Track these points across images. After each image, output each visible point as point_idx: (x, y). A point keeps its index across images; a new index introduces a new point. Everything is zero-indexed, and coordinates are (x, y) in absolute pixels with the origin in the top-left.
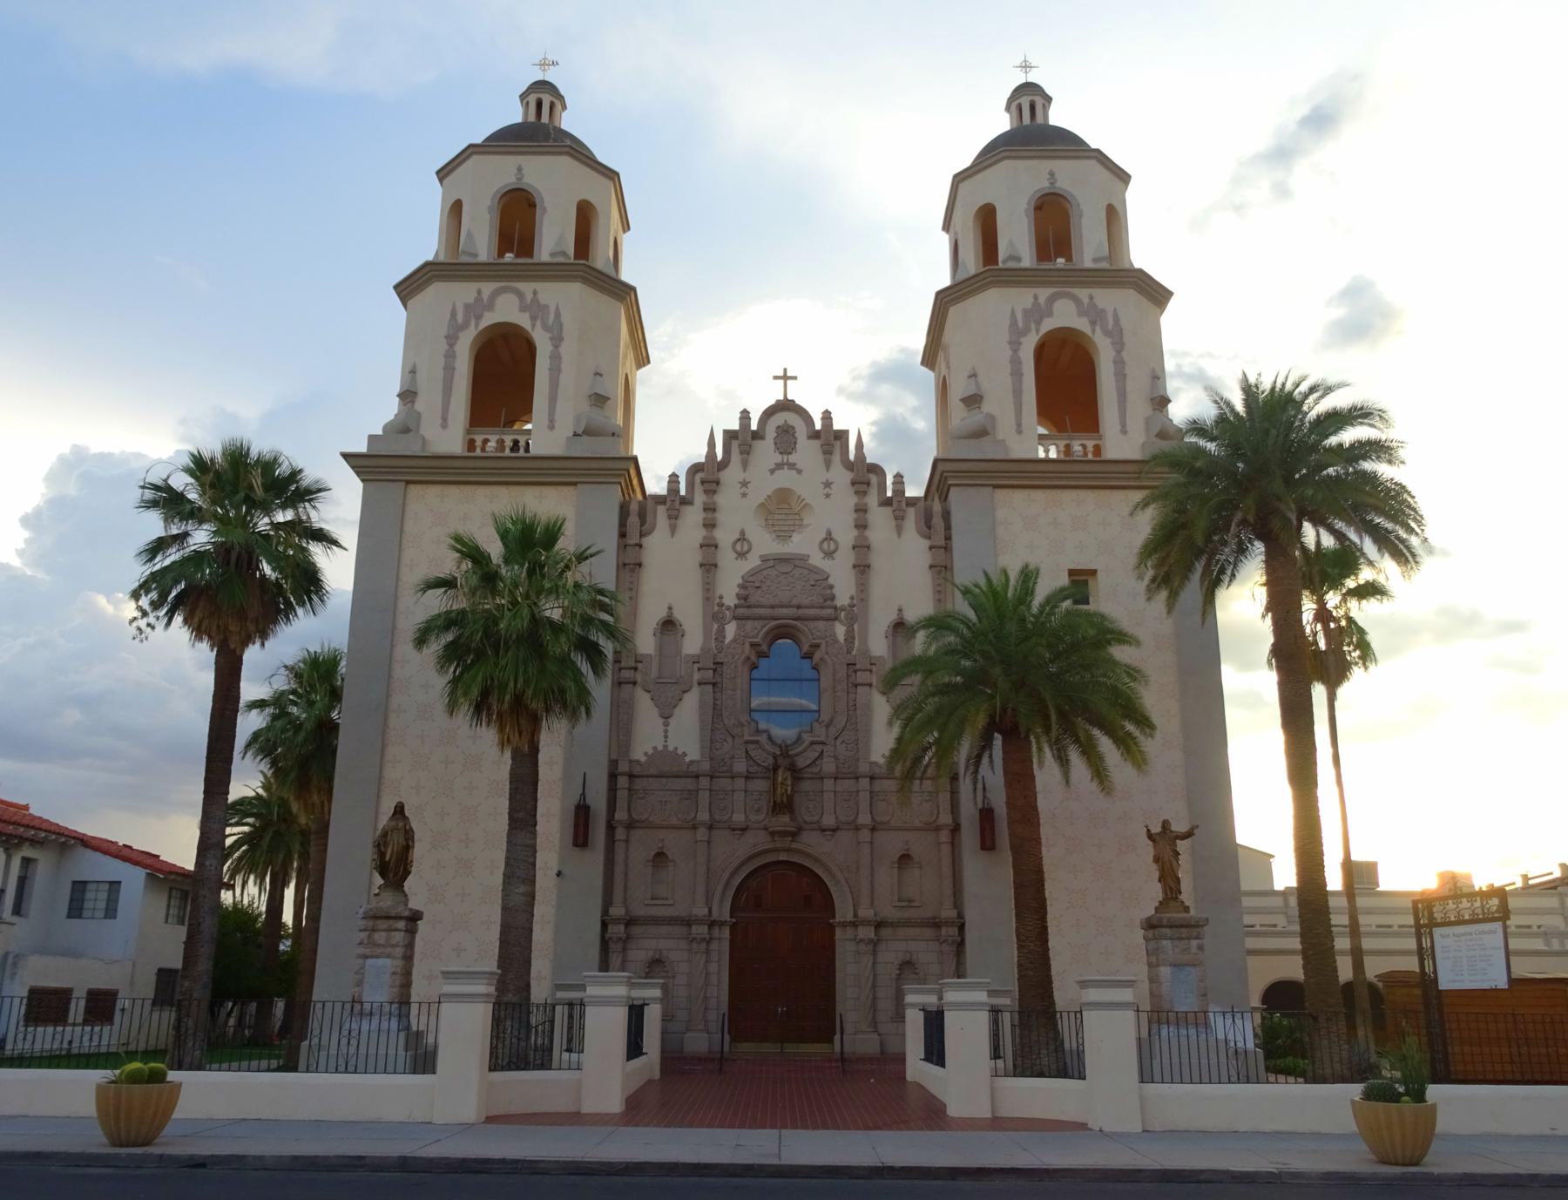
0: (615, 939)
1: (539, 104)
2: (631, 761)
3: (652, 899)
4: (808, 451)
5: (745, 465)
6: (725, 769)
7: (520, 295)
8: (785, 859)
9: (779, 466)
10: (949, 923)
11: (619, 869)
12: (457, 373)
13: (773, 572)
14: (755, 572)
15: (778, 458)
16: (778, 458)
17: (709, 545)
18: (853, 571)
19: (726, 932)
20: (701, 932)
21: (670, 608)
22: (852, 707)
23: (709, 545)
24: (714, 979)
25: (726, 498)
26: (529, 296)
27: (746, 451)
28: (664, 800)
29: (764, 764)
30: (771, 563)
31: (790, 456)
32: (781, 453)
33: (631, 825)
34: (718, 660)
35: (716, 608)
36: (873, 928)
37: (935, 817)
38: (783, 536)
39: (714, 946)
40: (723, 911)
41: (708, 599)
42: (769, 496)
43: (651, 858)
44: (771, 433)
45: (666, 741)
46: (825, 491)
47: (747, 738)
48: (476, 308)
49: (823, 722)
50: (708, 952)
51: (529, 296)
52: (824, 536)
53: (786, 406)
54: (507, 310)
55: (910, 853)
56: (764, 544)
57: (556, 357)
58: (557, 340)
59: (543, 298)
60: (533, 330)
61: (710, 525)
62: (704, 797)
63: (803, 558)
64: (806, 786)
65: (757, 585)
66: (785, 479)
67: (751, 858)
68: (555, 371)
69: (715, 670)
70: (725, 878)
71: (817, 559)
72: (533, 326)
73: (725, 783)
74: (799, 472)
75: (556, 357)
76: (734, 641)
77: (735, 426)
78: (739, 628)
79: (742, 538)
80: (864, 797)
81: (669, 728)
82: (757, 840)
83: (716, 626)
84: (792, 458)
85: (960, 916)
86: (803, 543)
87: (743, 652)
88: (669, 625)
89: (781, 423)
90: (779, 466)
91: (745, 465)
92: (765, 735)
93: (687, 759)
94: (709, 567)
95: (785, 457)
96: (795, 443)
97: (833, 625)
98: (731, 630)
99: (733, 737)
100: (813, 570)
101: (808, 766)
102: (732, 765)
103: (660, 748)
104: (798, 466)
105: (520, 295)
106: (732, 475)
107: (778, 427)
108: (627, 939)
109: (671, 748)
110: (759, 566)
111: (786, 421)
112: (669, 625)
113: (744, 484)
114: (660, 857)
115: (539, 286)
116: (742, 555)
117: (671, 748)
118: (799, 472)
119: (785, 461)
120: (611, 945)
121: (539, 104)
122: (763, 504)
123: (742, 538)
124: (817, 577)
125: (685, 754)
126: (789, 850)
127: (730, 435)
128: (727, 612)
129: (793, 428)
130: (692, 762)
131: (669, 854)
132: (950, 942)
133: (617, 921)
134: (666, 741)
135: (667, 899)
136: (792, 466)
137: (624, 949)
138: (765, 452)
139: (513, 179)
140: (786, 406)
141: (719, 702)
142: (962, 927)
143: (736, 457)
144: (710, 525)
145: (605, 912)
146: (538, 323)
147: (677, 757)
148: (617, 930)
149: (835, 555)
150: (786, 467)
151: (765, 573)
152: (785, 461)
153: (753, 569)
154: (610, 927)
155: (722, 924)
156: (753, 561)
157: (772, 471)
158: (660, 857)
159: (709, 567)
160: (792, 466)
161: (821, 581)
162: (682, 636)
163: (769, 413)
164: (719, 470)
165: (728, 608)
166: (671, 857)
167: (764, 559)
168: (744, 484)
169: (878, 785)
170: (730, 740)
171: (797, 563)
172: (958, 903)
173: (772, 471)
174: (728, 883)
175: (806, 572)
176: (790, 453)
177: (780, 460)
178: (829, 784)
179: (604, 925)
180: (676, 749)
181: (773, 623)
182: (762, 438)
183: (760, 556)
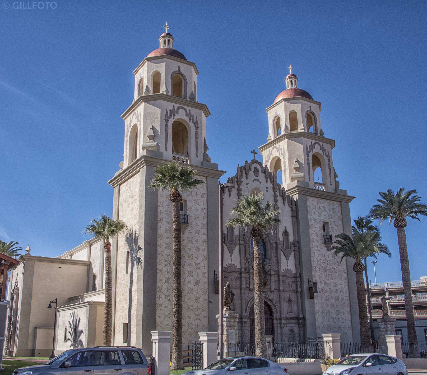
4: (262, 177)
9: (255, 180)
12: (310, 165)
16: (255, 177)
31: (258, 177)
32: (256, 176)
74: (260, 182)
81: (232, 257)
84: (258, 178)
99: (249, 262)
113: (247, 184)
118: (260, 182)
134: (231, 262)
136: (258, 180)
140: (255, 161)
157: (254, 181)
168: (247, 184)
170: (248, 263)
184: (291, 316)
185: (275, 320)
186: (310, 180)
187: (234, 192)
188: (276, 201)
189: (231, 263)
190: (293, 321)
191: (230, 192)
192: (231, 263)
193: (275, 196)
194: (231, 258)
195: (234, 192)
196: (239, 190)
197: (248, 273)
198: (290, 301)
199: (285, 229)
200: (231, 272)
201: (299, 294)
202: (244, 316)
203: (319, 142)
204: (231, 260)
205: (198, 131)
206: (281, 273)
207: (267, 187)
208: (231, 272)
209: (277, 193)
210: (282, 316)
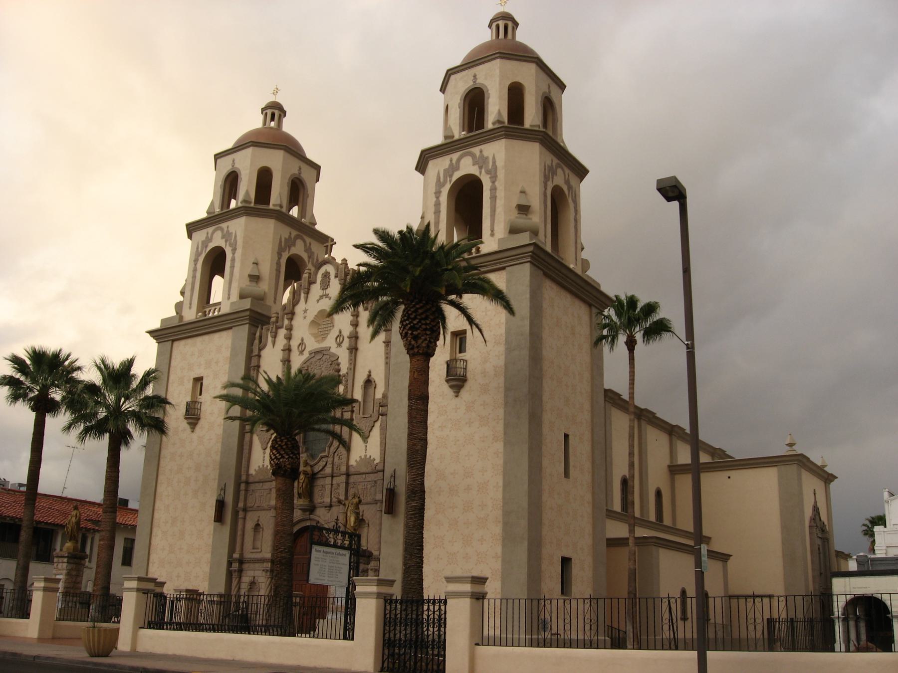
1: (498, 27)
3: (253, 549)
7: (473, 155)
9: (321, 297)
13: (314, 359)
15: (321, 293)
16: (321, 293)
17: (288, 350)
21: (370, 372)
23: (288, 350)
26: (478, 154)
30: (313, 355)
32: (322, 289)
33: (245, 510)
38: (324, 339)
41: (387, 363)
42: (316, 316)
43: (253, 527)
48: (454, 168)
51: (478, 154)
54: (467, 167)
56: (312, 345)
57: (493, 189)
58: (494, 179)
59: (485, 154)
60: (480, 175)
64: (320, 482)
65: (306, 368)
68: (494, 198)
71: (334, 349)
72: (481, 173)
75: (493, 189)
79: (302, 343)
84: (328, 291)
86: (330, 342)
88: (369, 382)
90: (321, 297)
96: (329, 282)
100: (334, 355)
103: (363, 457)
105: (473, 155)
106: (299, 309)
108: (240, 571)
110: (308, 357)
111: (326, 270)
112: (369, 382)
115: (483, 147)
121: (498, 27)
122: (313, 320)
123: (302, 343)
131: (260, 524)
133: (235, 560)
139: (472, 83)
144: (289, 338)
145: (230, 554)
146: (483, 171)
148: (235, 566)
150: (324, 297)
151: (311, 360)
153: (305, 360)
154: (233, 564)
156: (306, 355)
157: (318, 301)
161: (335, 362)
162: (375, 388)
166: (261, 526)
168: (305, 311)
171: (325, 353)
173: (318, 301)
175: (329, 357)
176: (327, 288)
178: (328, 480)
179: (230, 563)
180: (360, 457)
183: (309, 352)
189: (263, 465)
192: (263, 465)
196: (290, 329)
199: (369, 376)
204: (264, 460)
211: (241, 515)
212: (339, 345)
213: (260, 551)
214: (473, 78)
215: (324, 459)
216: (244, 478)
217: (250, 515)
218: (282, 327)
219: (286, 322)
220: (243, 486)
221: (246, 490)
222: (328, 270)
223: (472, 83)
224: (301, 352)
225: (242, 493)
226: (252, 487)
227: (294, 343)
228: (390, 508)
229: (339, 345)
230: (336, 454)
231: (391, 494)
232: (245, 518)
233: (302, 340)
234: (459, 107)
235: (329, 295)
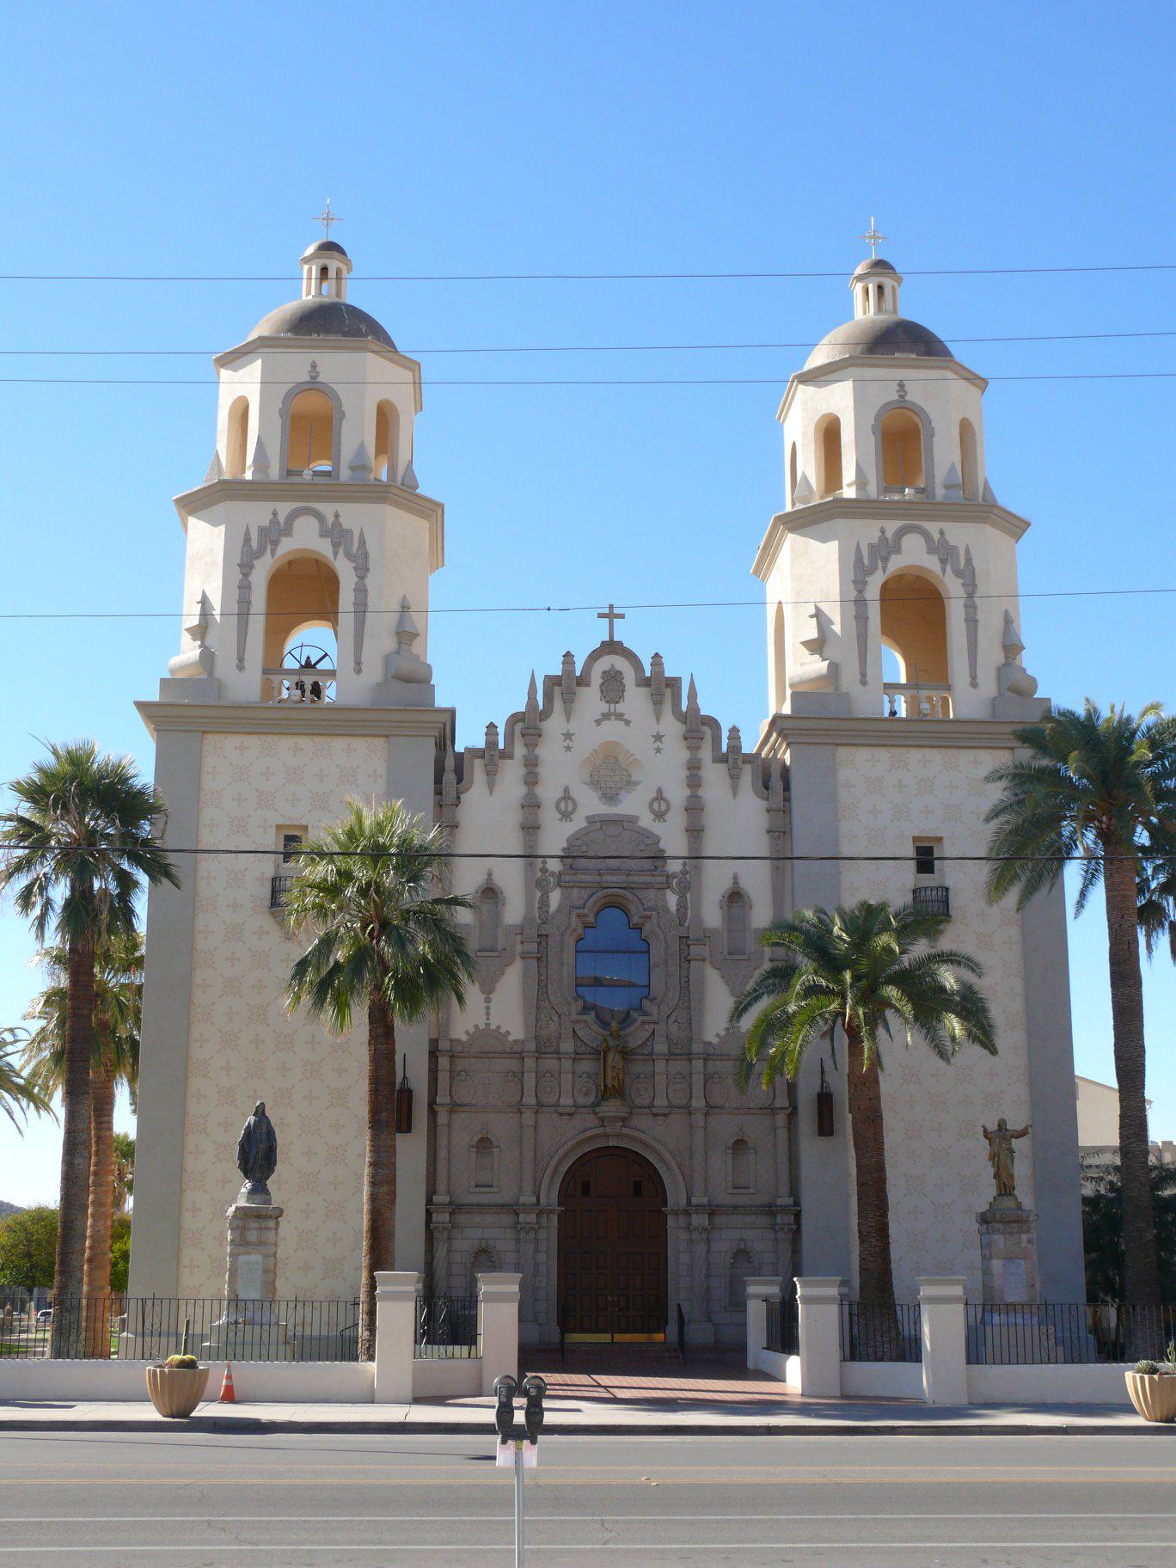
0: (440, 1229)
2: (451, 1040)
4: (635, 700)
5: (568, 715)
6: (552, 1050)
8: (615, 1144)
10: (784, 1209)
11: (442, 1154)
14: (577, 836)
16: (604, 707)
17: (531, 805)
18: (685, 834)
19: (555, 1219)
20: (529, 1220)
22: (685, 986)
23: (531, 805)
24: (543, 1269)
25: (550, 751)
27: (569, 700)
28: (487, 1082)
29: (591, 1045)
32: (608, 702)
33: (454, 1107)
34: (544, 932)
35: (540, 874)
36: (707, 1216)
37: (771, 1100)
39: (542, 1235)
40: (550, 1197)
43: (475, 1144)
44: (596, 679)
45: (488, 1019)
46: (656, 746)
47: (574, 1016)
49: (655, 999)
50: (537, 1241)
52: (654, 795)
53: (611, 647)
55: (745, 1138)
56: (590, 804)
61: (531, 779)
62: (530, 1080)
63: (633, 820)
64: (637, 1068)
66: (612, 729)
67: (579, 1144)
69: (539, 944)
70: (553, 1164)
71: (646, 821)
73: (550, 1063)
74: (628, 723)
76: (560, 910)
77: (557, 670)
78: (564, 898)
79: (567, 796)
80: (698, 1081)
82: (585, 1123)
83: (538, 894)
84: (620, 707)
85: (797, 1203)
86: (634, 804)
87: (569, 924)
89: (607, 668)
91: (568, 715)
92: (593, 1013)
93: (511, 1038)
94: (530, 828)
95: (612, 706)
96: (623, 691)
97: (664, 895)
98: (555, 898)
99: (560, 1016)
100: (646, 834)
101: (639, 1046)
102: (558, 1046)
104: (625, 717)
106: (554, 725)
107: (604, 673)
109: (493, 1027)
110: (584, 828)
113: (568, 736)
114: (484, 1144)
116: (566, 816)
117: (493, 1027)
118: (628, 723)
119: (612, 711)
120: (436, 1234)
122: (588, 758)
123: (567, 796)
124: (648, 842)
125: (508, 1033)
126: (618, 1136)
127: (552, 682)
128: (551, 879)
129: (620, 673)
130: (515, 1041)
131: (493, 1139)
132: (786, 1230)
134: (488, 1019)
135: (492, 1186)
136: (620, 716)
137: (449, 1239)
138: (591, 700)
140: (611, 647)
141: (543, 978)
142: (798, 1215)
143: (558, 705)
144: (531, 779)
145: (429, 1201)
147: (499, 1035)
149: (666, 817)
150: (613, 717)
152: (612, 711)
155: (550, 1212)
156: (578, 823)
157: (598, 722)
158: (484, 1144)
159: (530, 828)
160: (620, 716)
163: (595, 656)
164: (541, 721)
165: (553, 874)
166: (495, 1143)
167: (591, 820)
168: (568, 736)
169: (712, 1066)
170: (556, 1018)
171: (626, 825)
172: (794, 1191)
173: (598, 722)
174: (555, 1172)
176: (617, 702)
177: (606, 711)
179: (429, 1214)
181: (601, 894)
182: (588, 685)
183: (587, 818)
184: (741, 1200)
185: (669, 1217)
186: (864, 682)
187: (512, 772)
188: (694, 782)
189: (488, 1025)
190: (749, 1219)
191: (491, 774)
192: (488, 1025)
193: (694, 767)
194: (488, 1008)
195: (512, 772)
196: (531, 764)
197: (555, 1056)
198: (739, 1145)
199: (736, 882)
200: (485, 1055)
201: (781, 1119)
202: (524, 1205)
203: (917, 523)
204: (488, 1014)
205: (369, 581)
206: (697, 1048)
207: (658, 738)
208: (485, 1055)
209: (706, 754)
210: (694, 1201)
211: (442, 1118)
212: (660, 816)
213: (497, 1190)
214: (898, 388)
215: (646, 1026)
216: (444, 1045)
217: (460, 1118)
218: (511, 757)
219: (520, 751)
220: (443, 1062)
221: (453, 1073)
222: (618, 667)
223: (897, 398)
224: (566, 816)
225: (443, 1077)
226: (460, 1064)
227: (549, 792)
228: (826, 1127)
229: (660, 816)
230: (671, 1021)
231: (825, 1101)
232: (449, 1126)
233: (567, 790)
234: (874, 433)
235: (625, 717)
